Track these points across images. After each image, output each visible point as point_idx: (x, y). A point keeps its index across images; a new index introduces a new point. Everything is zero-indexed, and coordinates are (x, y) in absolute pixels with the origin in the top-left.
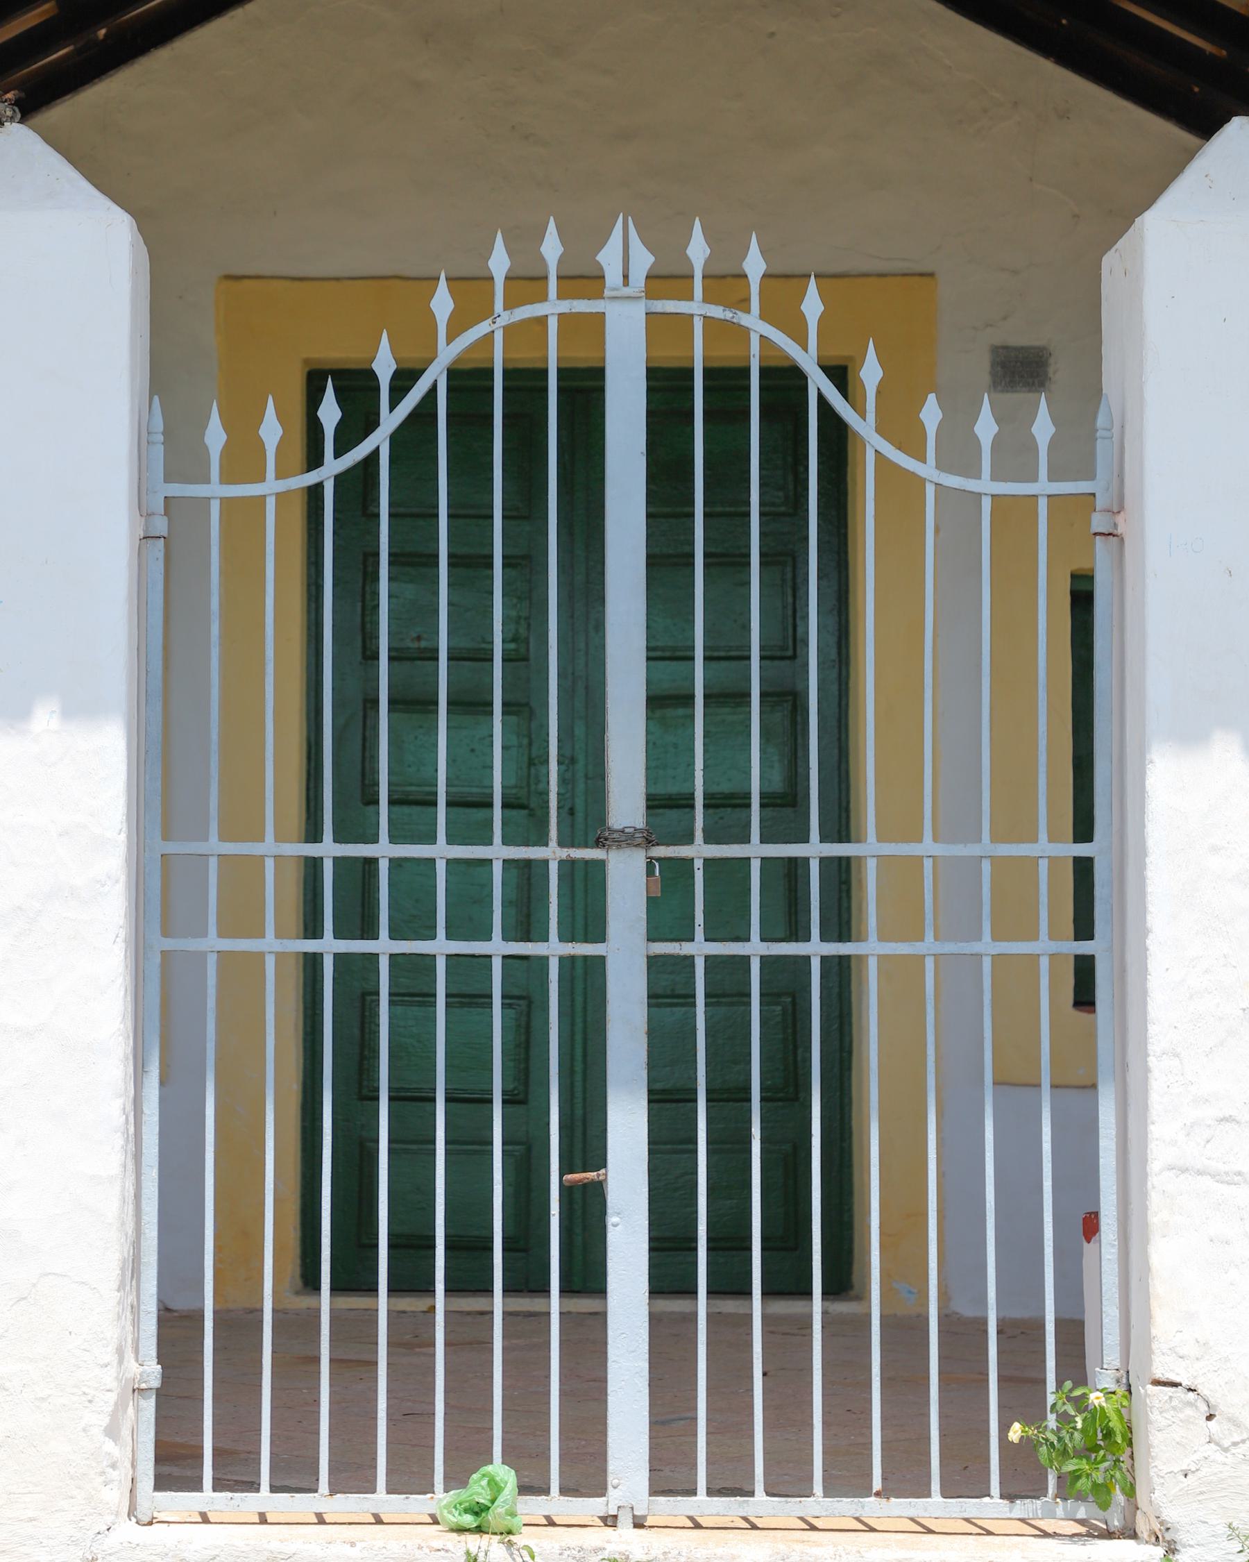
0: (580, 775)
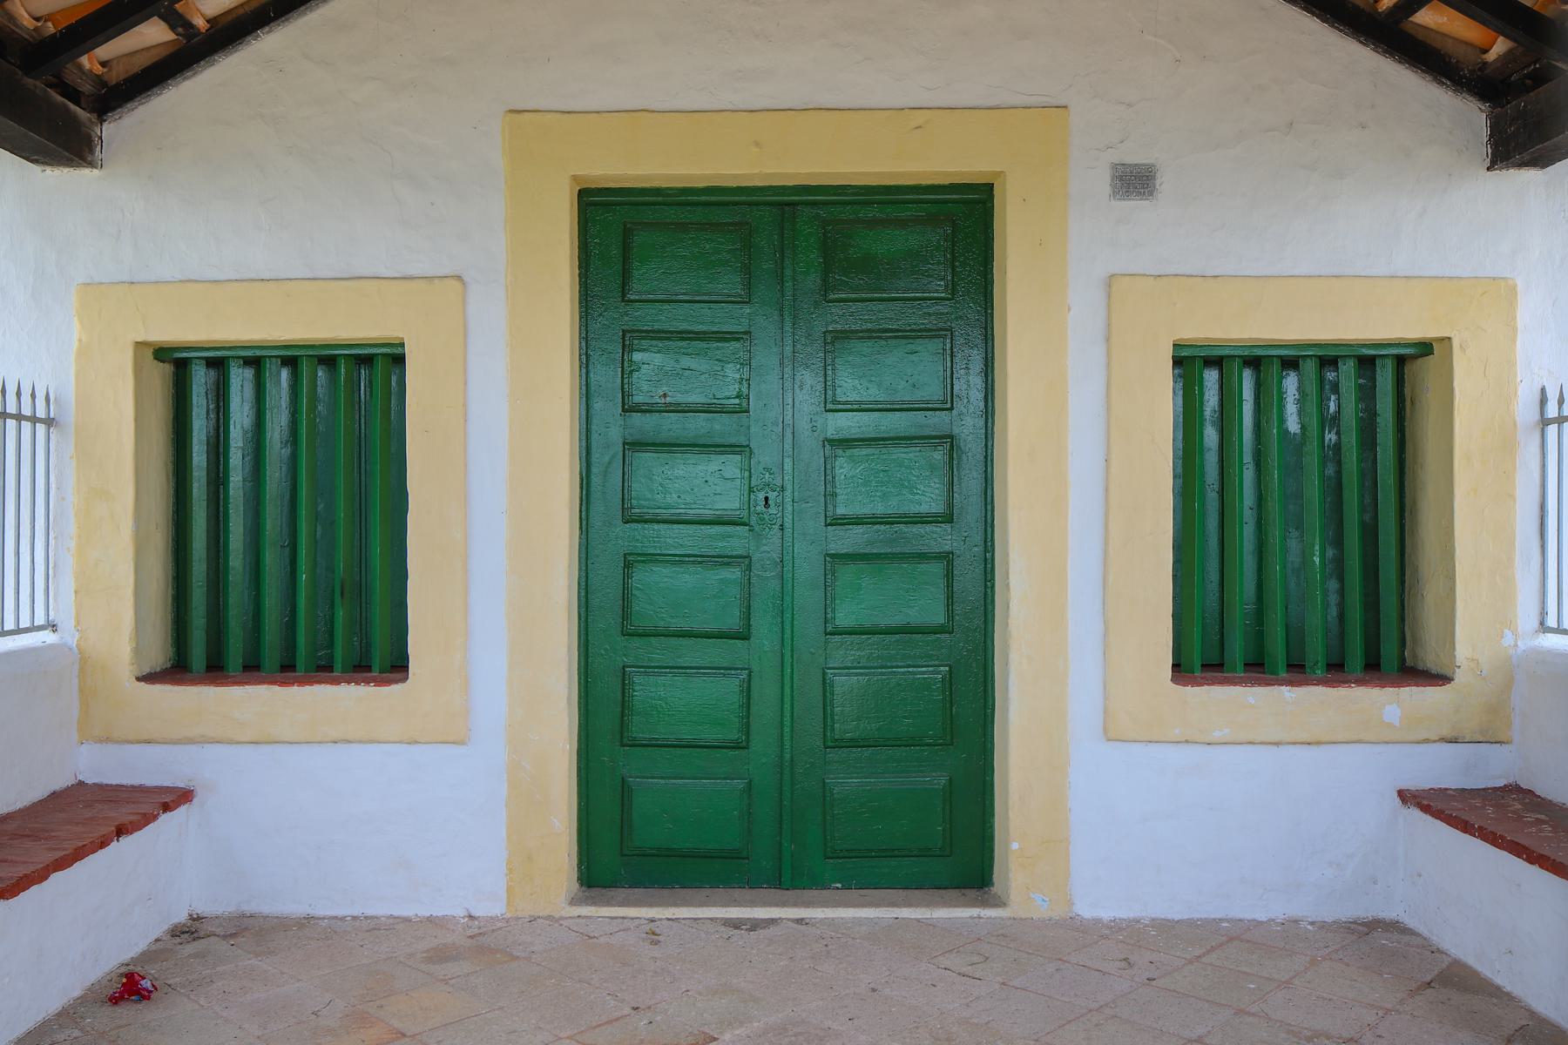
0: (788, 499)
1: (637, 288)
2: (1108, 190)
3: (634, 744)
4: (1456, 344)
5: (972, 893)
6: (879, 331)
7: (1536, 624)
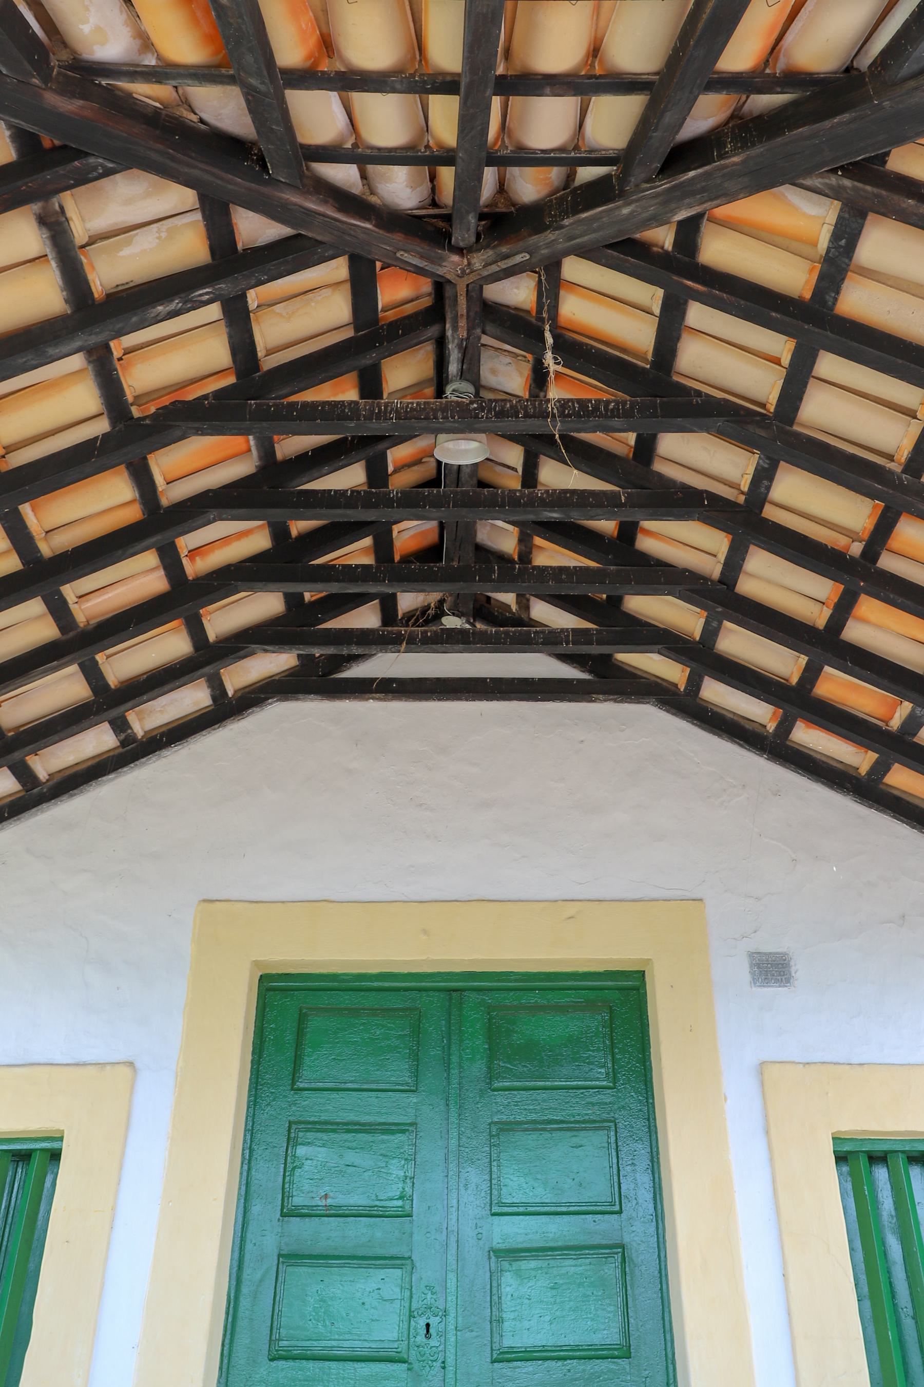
2: (747, 977)
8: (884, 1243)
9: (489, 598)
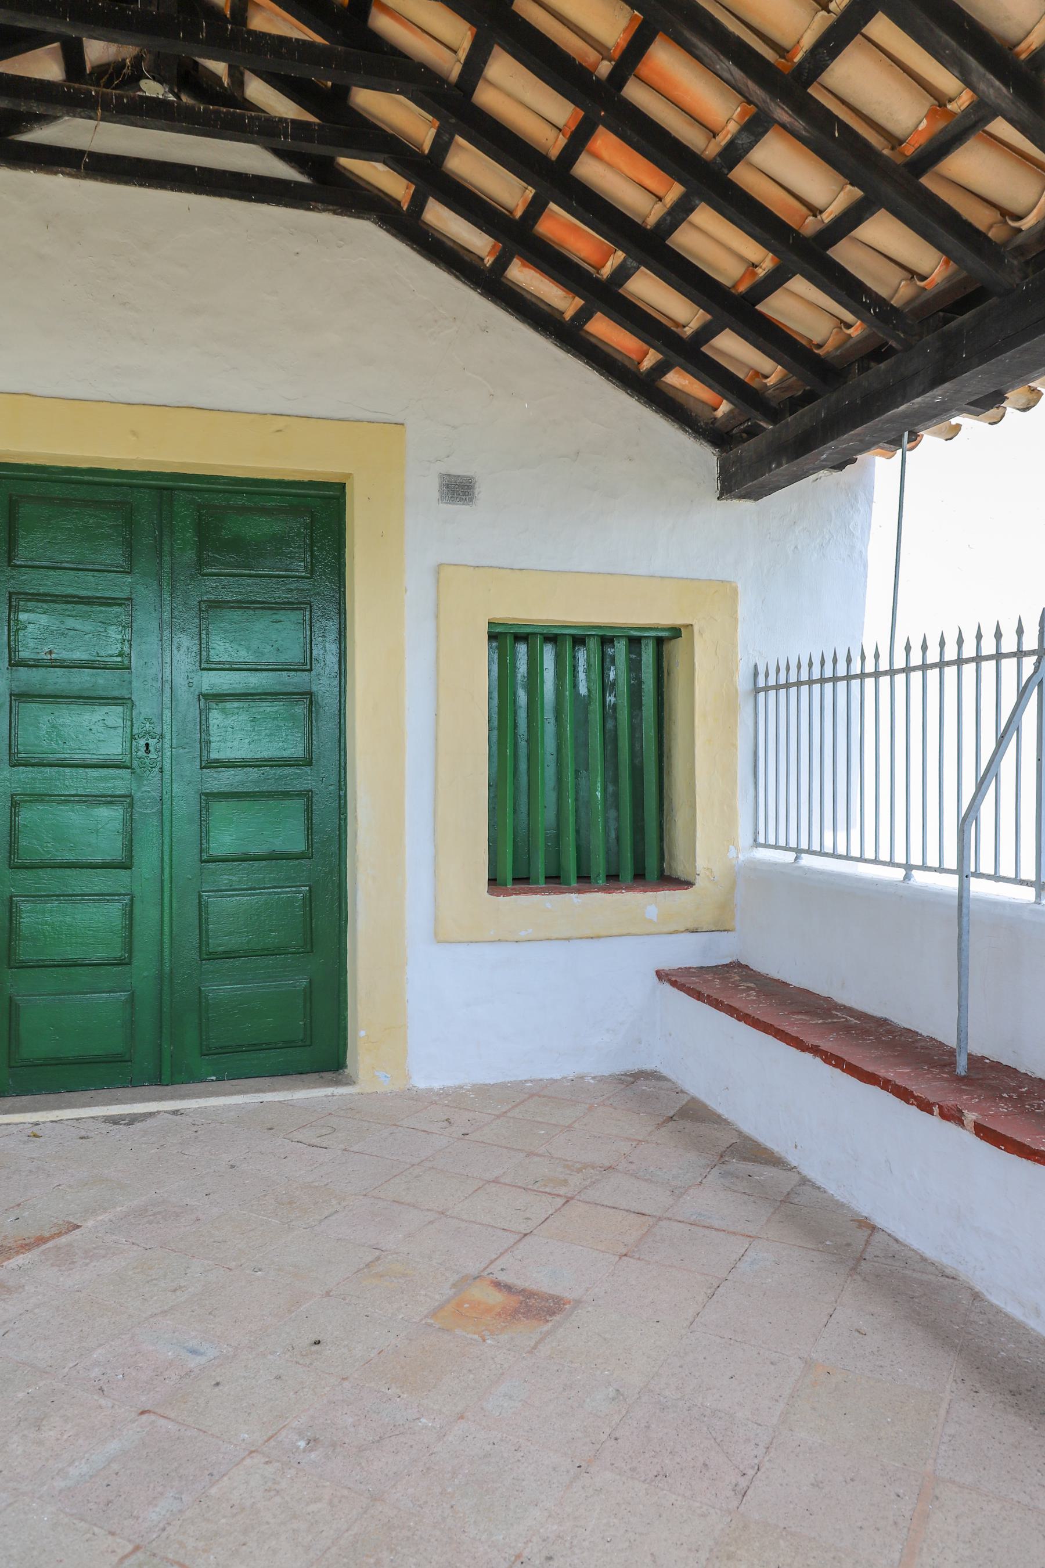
0: (167, 746)
1: (24, 553)
3: (23, 966)
4: (696, 629)
5: (328, 1075)
6: (248, 602)
7: (752, 841)
8: (515, 694)
9: (196, 63)
